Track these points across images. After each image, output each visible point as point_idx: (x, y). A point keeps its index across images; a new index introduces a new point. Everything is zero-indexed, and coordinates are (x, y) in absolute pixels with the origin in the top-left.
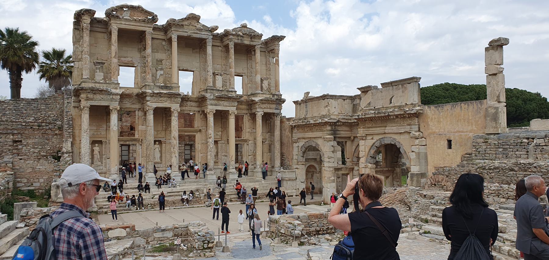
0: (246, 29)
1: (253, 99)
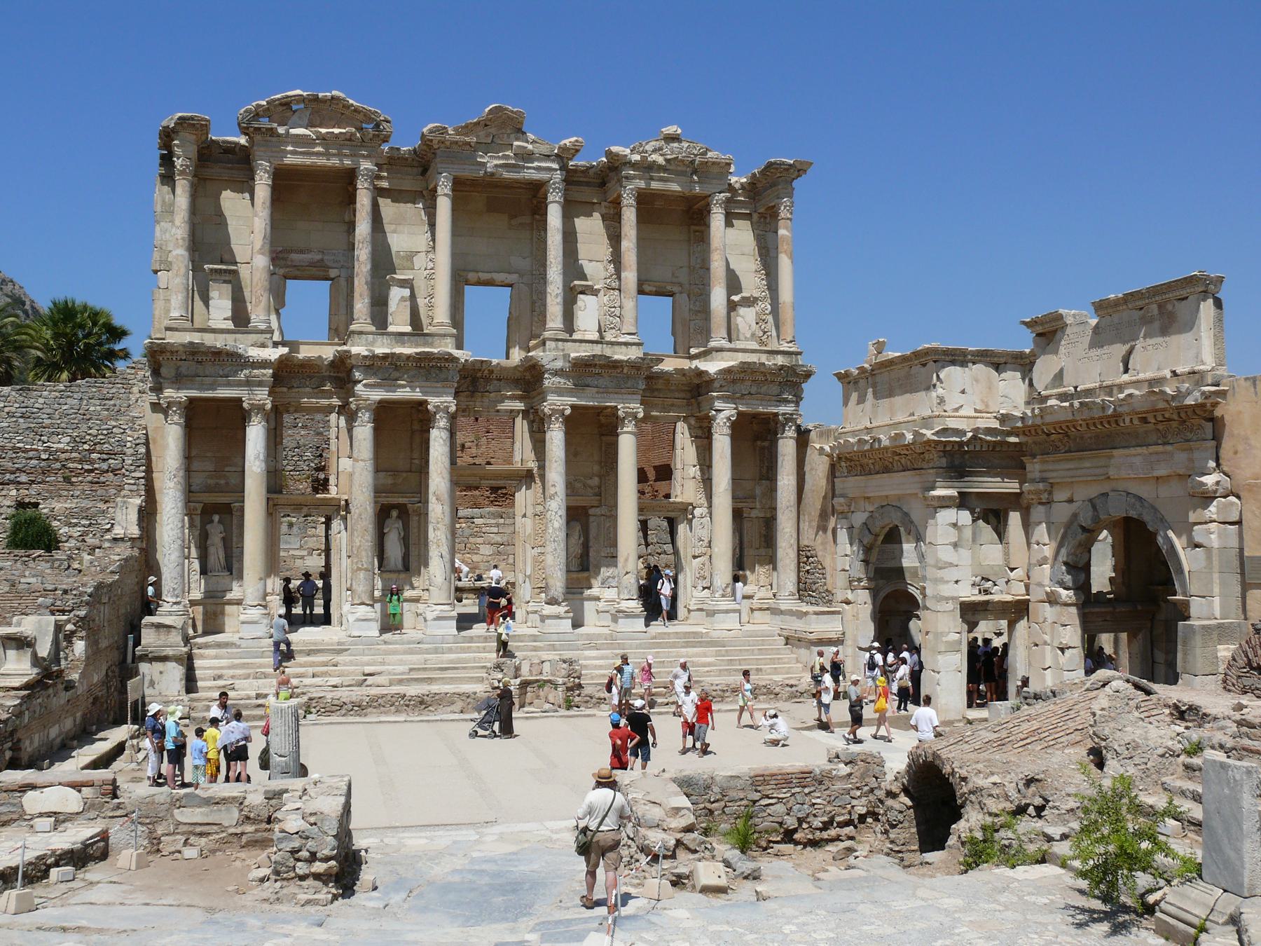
1: (703, 365)
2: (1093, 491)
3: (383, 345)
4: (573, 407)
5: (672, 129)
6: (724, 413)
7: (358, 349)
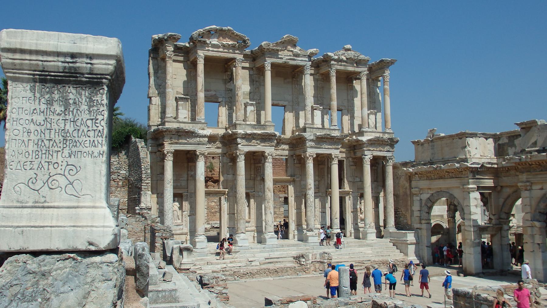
0: (349, 52)
1: (360, 138)
3: (248, 130)
4: (317, 154)
5: (348, 46)
6: (368, 156)
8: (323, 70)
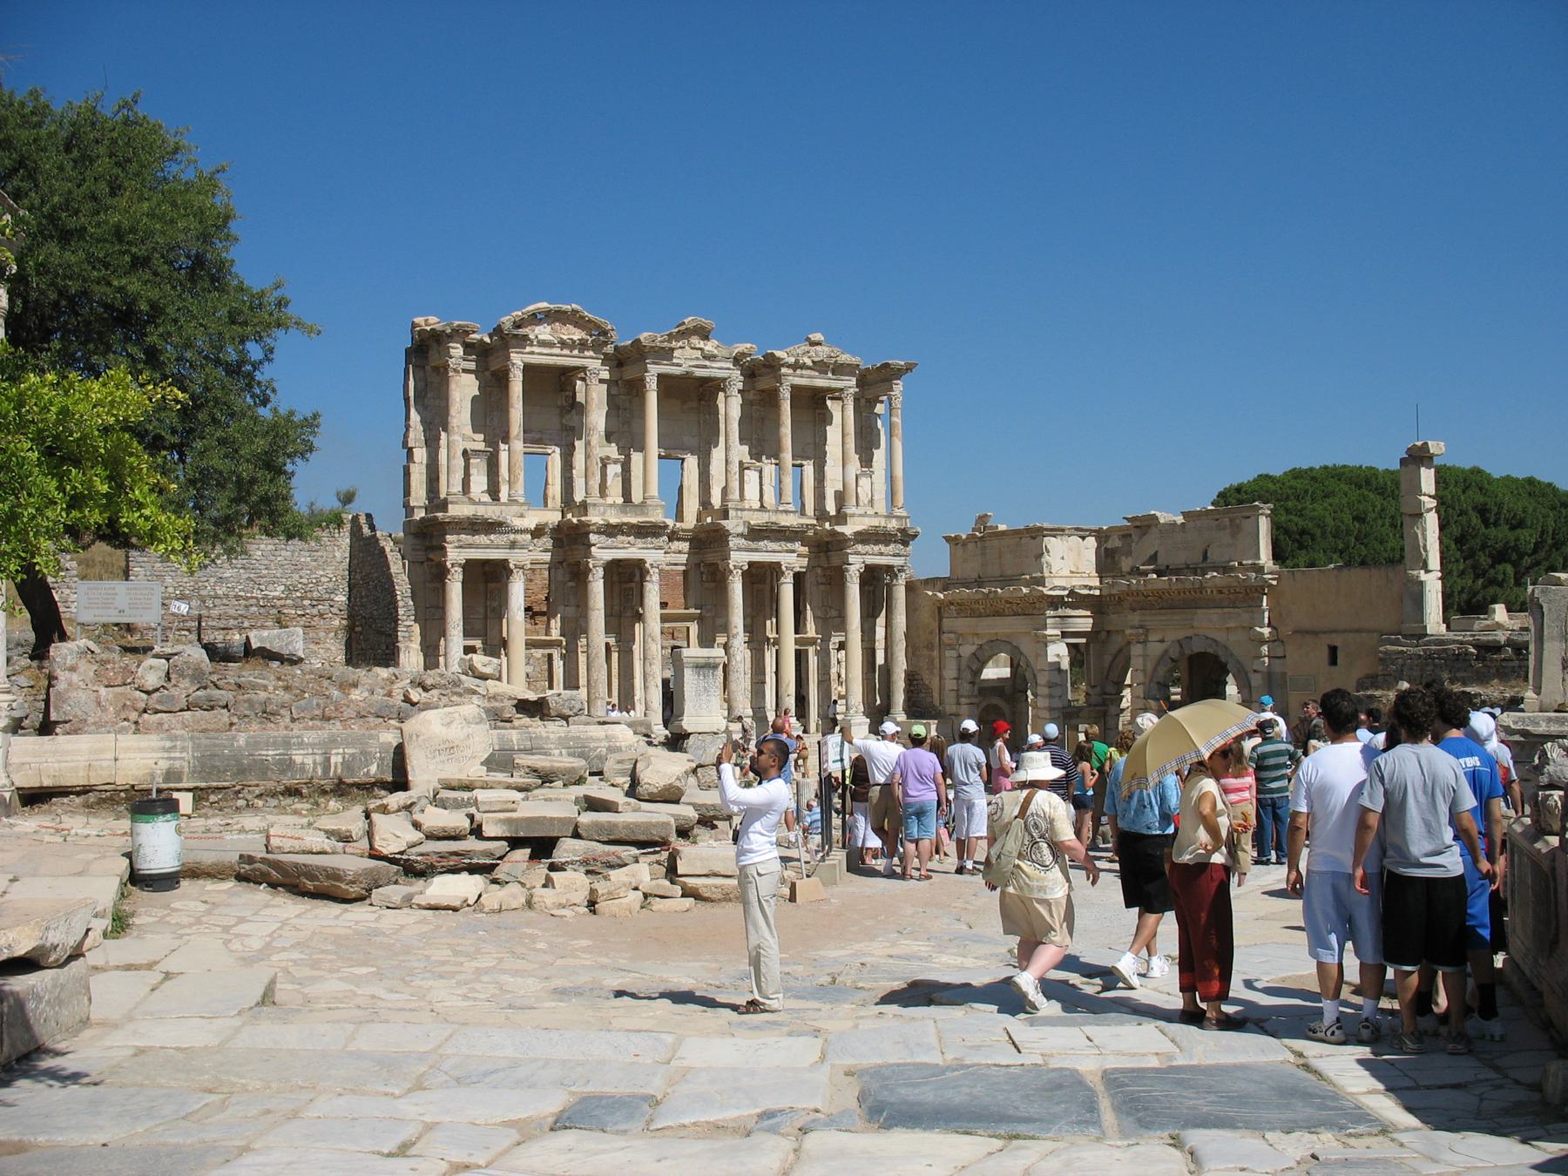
0: (818, 348)
1: (839, 529)
2: (1181, 635)
5: (818, 337)
7: (595, 518)
8: (764, 383)
